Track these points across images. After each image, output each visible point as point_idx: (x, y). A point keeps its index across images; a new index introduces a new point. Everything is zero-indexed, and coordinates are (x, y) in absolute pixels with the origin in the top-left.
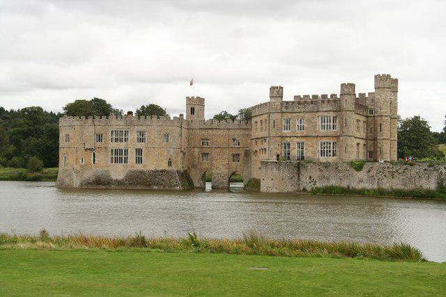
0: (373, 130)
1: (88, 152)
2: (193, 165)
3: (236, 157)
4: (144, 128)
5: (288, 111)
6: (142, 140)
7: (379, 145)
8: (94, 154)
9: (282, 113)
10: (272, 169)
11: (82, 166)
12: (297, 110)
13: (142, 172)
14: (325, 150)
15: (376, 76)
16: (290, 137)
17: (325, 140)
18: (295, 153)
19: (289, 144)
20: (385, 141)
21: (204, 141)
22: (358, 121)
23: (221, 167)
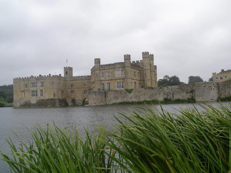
0: (143, 76)
1: (22, 92)
2: (68, 96)
3: (85, 91)
4: (43, 81)
5: (103, 69)
6: (42, 86)
7: (145, 83)
8: (24, 93)
9: (100, 70)
10: (92, 95)
11: (20, 98)
12: (106, 68)
13: (43, 100)
14: (119, 85)
15: (142, 53)
16: (104, 81)
17: (118, 81)
18: (106, 87)
19: (104, 84)
20: (148, 81)
21: (72, 86)
22: (135, 72)
23: (79, 96)
